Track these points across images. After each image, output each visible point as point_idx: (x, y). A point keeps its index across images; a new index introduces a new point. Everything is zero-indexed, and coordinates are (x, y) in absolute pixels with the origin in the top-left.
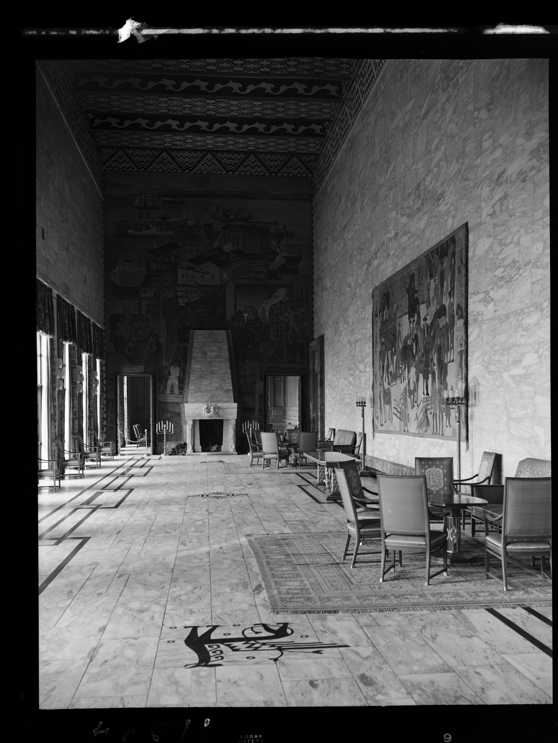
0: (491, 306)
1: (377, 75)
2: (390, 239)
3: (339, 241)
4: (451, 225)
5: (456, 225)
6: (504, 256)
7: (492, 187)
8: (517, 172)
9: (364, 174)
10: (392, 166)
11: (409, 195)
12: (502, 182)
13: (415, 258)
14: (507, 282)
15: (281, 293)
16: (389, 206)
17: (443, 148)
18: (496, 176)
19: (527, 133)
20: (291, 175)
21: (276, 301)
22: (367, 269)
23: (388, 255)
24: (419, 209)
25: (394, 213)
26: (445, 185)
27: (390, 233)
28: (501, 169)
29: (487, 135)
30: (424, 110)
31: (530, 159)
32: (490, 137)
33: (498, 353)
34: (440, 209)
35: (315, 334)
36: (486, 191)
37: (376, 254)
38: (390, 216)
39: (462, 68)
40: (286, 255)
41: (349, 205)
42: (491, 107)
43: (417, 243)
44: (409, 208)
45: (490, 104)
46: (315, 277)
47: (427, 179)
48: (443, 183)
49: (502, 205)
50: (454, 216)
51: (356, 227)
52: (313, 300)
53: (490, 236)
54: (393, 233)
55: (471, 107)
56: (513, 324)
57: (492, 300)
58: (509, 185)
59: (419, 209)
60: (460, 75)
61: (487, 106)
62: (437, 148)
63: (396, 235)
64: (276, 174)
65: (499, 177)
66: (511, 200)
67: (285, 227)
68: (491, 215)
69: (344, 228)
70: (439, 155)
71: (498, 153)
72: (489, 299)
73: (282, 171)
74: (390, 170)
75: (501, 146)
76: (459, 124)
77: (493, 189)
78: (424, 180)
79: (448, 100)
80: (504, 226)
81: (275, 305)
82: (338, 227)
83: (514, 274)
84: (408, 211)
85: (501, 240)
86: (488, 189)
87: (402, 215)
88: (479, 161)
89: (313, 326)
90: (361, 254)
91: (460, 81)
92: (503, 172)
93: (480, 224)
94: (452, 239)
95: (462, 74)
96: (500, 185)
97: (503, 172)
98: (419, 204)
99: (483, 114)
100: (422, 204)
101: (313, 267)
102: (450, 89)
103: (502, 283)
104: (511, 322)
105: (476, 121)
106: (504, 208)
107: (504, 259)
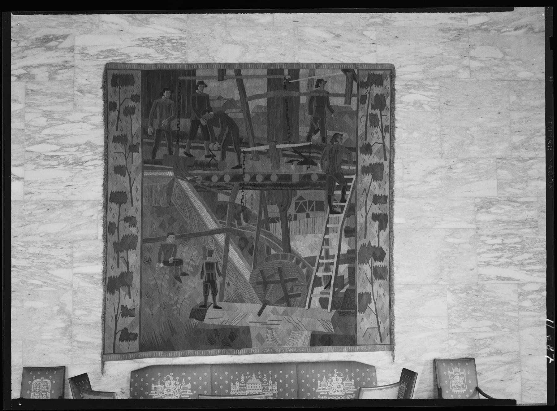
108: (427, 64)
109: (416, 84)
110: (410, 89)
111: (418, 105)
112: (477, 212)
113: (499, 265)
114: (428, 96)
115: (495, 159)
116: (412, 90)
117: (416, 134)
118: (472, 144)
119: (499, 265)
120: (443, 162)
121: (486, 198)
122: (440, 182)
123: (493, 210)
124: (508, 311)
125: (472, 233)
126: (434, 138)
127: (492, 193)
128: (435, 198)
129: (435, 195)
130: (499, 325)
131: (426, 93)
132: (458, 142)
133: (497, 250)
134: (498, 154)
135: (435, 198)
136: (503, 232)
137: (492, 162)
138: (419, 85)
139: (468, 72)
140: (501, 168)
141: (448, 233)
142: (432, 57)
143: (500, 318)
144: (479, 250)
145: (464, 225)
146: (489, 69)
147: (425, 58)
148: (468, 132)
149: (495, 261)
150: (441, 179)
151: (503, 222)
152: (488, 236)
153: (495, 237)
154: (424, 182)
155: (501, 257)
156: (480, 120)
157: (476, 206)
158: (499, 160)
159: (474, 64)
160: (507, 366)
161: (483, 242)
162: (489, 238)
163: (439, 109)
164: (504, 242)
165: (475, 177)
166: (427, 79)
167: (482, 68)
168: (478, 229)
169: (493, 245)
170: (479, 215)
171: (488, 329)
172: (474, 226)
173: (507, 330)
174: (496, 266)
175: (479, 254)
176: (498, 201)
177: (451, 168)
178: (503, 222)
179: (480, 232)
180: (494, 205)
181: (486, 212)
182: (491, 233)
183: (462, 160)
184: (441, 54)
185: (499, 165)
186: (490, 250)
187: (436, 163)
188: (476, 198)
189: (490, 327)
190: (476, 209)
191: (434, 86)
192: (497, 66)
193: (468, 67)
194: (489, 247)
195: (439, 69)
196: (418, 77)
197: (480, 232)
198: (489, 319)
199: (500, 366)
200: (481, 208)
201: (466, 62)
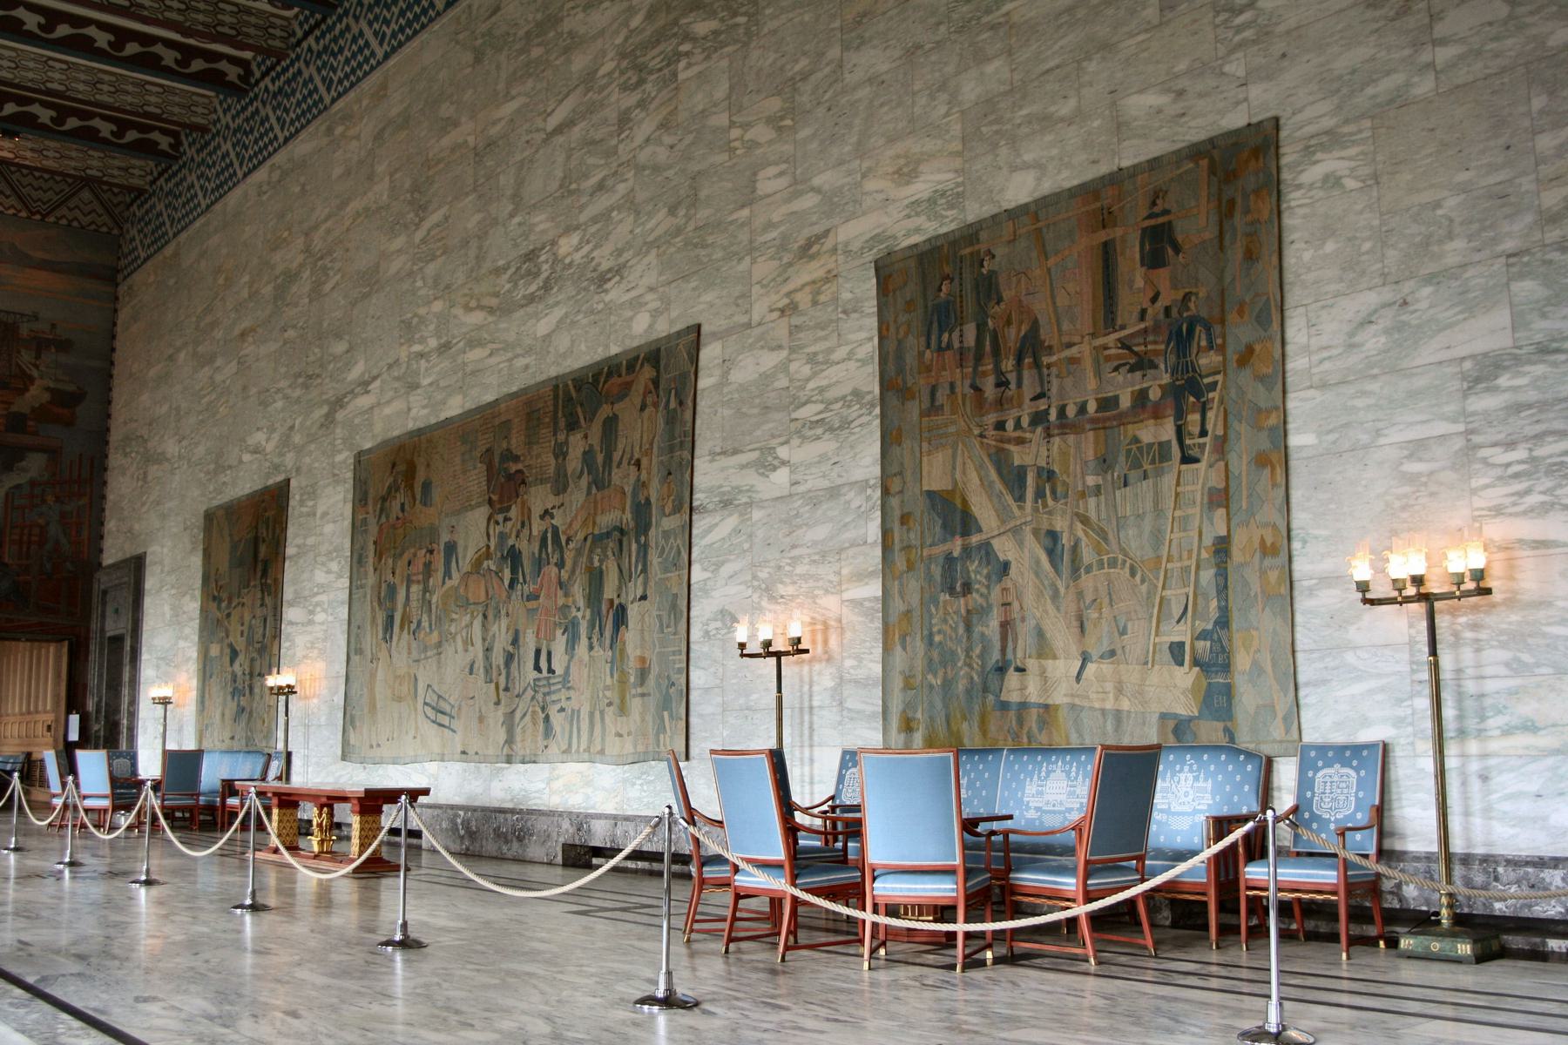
0: (781, 477)
1: (387, 56)
2: (421, 355)
3: (219, 362)
4: (642, 327)
5: (663, 328)
6: (824, 383)
7: (785, 260)
8: (868, 236)
9: (328, 231)
10: (435, 218)
11: (498, 271)
12: (818, 253)
13: (514, 389)
14: (831, 430)
15: (34, 465)
16: (422, 292)
17: (622, 188)
18: (802, 242)
19: (898, 172)
20: (75, 224)
21: (22, 479)
22: (327, 416)
23: (415, 386)
24: (531, 299)
25: (438, 306)
26: (626, 256)
27: (423, 340)
28: (818, 229)
29: (772, 171)
30: (553, 122)
31: (909, 216)
32: (781, 174)
33: (806, 561)
34: (607, 298)
35: (105, 555)
36: (764, 268)
37: (367, 383)
38: (422, 311)
39: (687, 54)
40: (52, 385)
41: (267, 290)
42: (788, 122)
43: (520, 363)
44: (497, 295)
45: (782, 118)
46: (115, 437)
47: (562, 241)
48: (619, 252)
49: (818, 293)
50: (655, 314)
51: (291, 333)
52: (105, 483)
53: (780, 347)
54: (433, 343)
55: (721, 120)
56: (854, 505)
57: (784, 463)
58: (841, 258)
59: (531, 299)
60: (682, 65)
61: (773, 121)
62: (600, 187)
63: (445, 347)
64: (44, 216)
65: (809, 244)
66: (848, 286)
67: (53, 326)
68: (782, 311)
69: (243, 335)
70: (603, 202)
71: (809, 201)
72: (776, 463)
73: (58, 213)
74: (427, 224)
75: (818, 190)
76: (681, 146)
77: (790, 264)
78: (554, 243)
79: (642, 104)
80: (823, 329)
81: (18, 487)
82: (218, 334)
83: (855, 415)
84: (494, 302)
85: (815, 354)
86: (776, 263)
87: (468, 309)
88: (745, 212)
89: (102, 537)
90: (306, 386)
91: (682, 76)
92: (827, 233)
93: (749, 325)
94: (653, 356)
95: (689, 65)
96: (812, 257)
97: (827, 233)
98: (533, 288)
99: (761, 133)
100: (547, 287)
101: (109, 416)
102: (648, 86)
103: (819, 431)
104: (848, 502)
105: (736, 144)
106: (822, 298)
107: (822, 390)
108: (1344, 91)
109: (1325, 139)
110: (1314, 153)
111: (1332, 182)
112: (1466, 394)
113: (1525, 513)
114: (1350, 159)
115: (1503, 260)
116: (1319, 156)
117: (1330, 247)
118: (1450, 236)
119: (1525, 513)
120: (1387, 294)
121: (1485, 355)
122: (1383, 339)
123: (1504, 381)
124: (1549, 624)
125: (1459, 443)
126: (1367, 246)
127: (1502, 341)
128: (1375, 377)
129: (1376, 371)
130: (1526, 657)
131: (1344, 153)
132: (1418, 239)
133: (1516, 476)
134: (1509, 245)
135: (1375, 377)
136: (1531, 430)
137: (1495, 268)
138: (1332, 139)
139: (1431, 76)
140: (1522, 276)
141: (1406, 453)
142: (1353, 72)
143: (1530, 641)
144: (1475, 483)
145: (1442, 428)
146: (1479, 53)
147: (1340, 77)
148: (1440, 212)
149: (1515, 504)
150: (1387, 332)
151: (1530, 406)
152: (1494, 445)
153: (1510, 445)
154: (1352, 346)
155: (1528, 492)
156: (1463, 177)
157: (1464, 379)
158: (1512, 260)
159: (1443, 55)
160: (1550, 761)
161: (1485, 461)
162: (1498, 450)
163: (1376, 177)
164: (1535, 454)
165: (1461, 312)
166: (1347, 122)
167: (1461, 57)
168: (1472, 432)
169: (1508, 465)
170: (1472, 399)
171: (1503, 671)
172: (1461, 427)
173: (1544, 670)
174: (1516, 515)
175: (1474, 492)
176: (1516, 358)
177: (1405, 303)
178: (1530, 406)
179: (1476, 439)
180: (1506, 368)
181: (1488, 390)
182: (1502, 436)
183: (1430, 279)
184: (1373, 59)
185: (1514, 270)
186: (1500, 478)
187: (1372, 299)
188: (1463, 359)
189: (1507, 665)
190: (1465, 385)
191: (1360, 131)
192: (1496, 39)
193: (1431, 65)
194: (1499, 471)
195: (1370, 91)
196: (1328, 123)
197: (1476, 439)
198: (1503, 646)
199: (1535, 758)
200: (1478, 380)
201: (1425, 57)
